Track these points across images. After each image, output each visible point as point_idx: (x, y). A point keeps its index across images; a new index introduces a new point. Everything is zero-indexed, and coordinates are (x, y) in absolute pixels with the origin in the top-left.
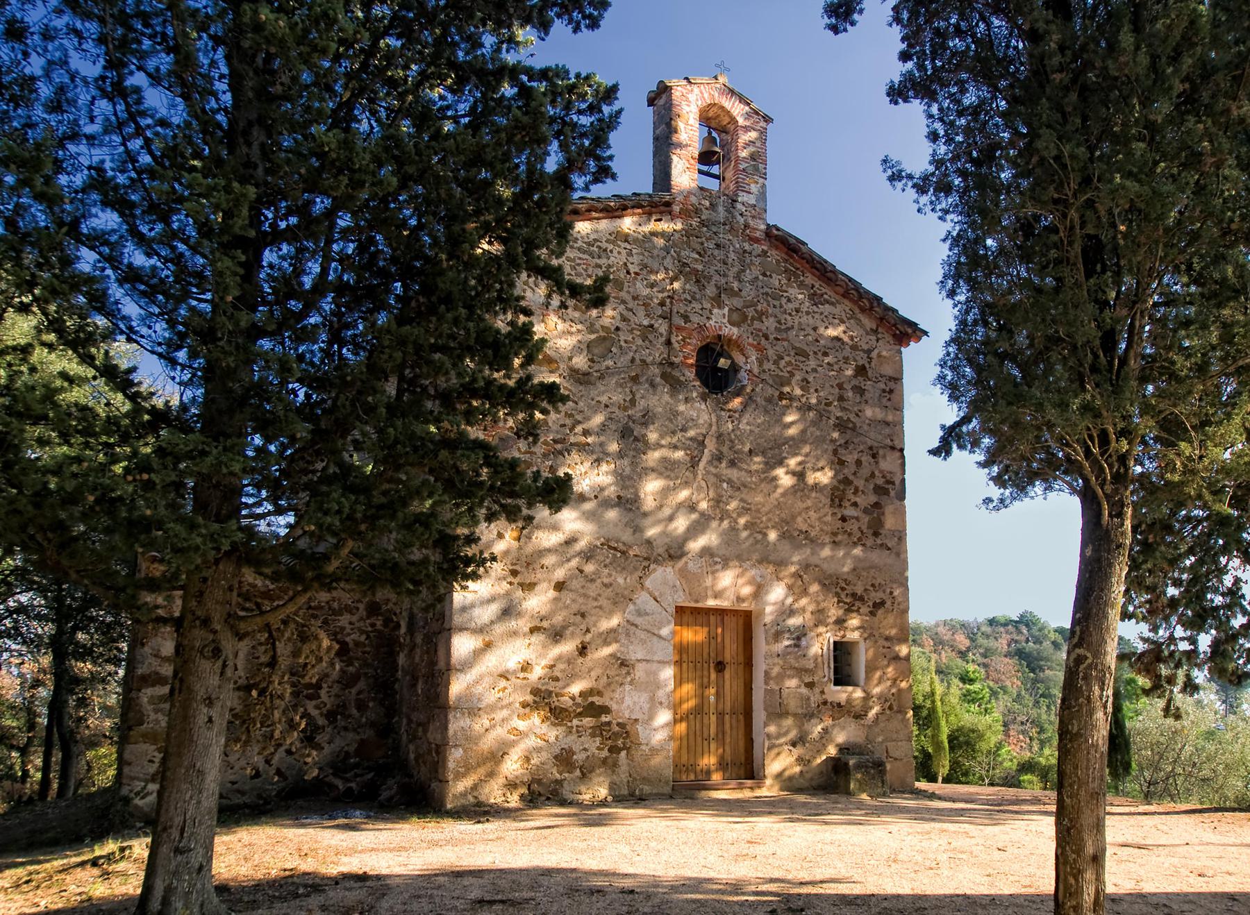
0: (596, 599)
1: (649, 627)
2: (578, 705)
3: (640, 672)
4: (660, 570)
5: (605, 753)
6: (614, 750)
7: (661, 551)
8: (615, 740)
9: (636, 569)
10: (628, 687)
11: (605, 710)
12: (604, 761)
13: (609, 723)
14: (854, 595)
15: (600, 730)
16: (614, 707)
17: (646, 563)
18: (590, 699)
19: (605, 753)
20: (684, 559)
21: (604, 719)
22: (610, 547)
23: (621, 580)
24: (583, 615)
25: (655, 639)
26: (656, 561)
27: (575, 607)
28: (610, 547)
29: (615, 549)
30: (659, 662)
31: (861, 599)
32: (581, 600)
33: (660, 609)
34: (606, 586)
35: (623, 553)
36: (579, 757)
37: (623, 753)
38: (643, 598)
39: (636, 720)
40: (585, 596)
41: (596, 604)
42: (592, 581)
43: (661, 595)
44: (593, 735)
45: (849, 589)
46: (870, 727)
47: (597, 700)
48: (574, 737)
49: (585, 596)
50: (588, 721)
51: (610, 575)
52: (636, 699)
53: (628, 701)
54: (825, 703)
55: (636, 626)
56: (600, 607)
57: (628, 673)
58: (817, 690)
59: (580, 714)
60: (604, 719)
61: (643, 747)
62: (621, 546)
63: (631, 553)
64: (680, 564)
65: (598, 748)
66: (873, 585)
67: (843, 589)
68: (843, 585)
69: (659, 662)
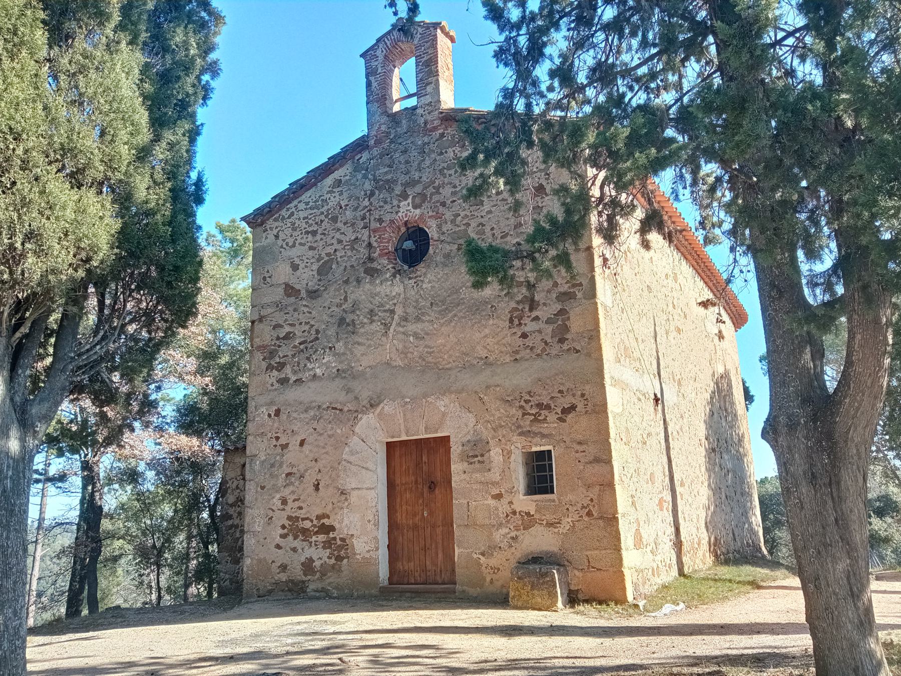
0: (324, 448)
1: (360, 463)
2: (315, 526)
3: (354, 497)
4: (365, 417)
5: (333, 561)
6: (339, 559)
7: (365, 402)
8: (339, 552)
9: (349, 420)
10: (346, 511)
11: (332, 528)
12: (333, 566)
13: (335, 539)
14: (540, 406)
15: (328, 544)
16: (337, 526)
17: (356, 414)
18: (322, 521)
19: (333, 561)
20: (382, 405)
21: (331, 535)
22: (333, 408)
23: (339, 431)
24: (316, 460)
25: (364, 471)
26: (363, 412)
27: (311, 456)
28: (333, 408)
29: (336, 409)
30: (367, 489)
31: (548, 407)
32: (315, 450)
33: (367, 447)
34: (330, 436)
35: (341, 410)
36: (317, 564)
37: (345, 561)
38: (355, 441)
39: (352, 535)
40: (318, 446)
41: (324, 451)
42: (321, 435)
43: (366, 436)
44: (324, 548)
45: (535, 400)
46: (565, 535)
47: (326, 521)
48: (313, 549)
49: (318, 446)
50: (322, 538)
51: (332, 428)
52: (351, 519)
53: (346, 521)
54: (514, 513)
55: (351, 463)
56: (327, 453)
57: (346, 499)
58: (504, 501)
59: (316, 533)
60: (331, 535)
61: (358, 557)
62: (339, 406)
63: (346, 409)
64: (379, 409)
65: (329, 558)
66: (560, 392)
67: (527, 402)
68: (528, 398)
69: (367, 489)
